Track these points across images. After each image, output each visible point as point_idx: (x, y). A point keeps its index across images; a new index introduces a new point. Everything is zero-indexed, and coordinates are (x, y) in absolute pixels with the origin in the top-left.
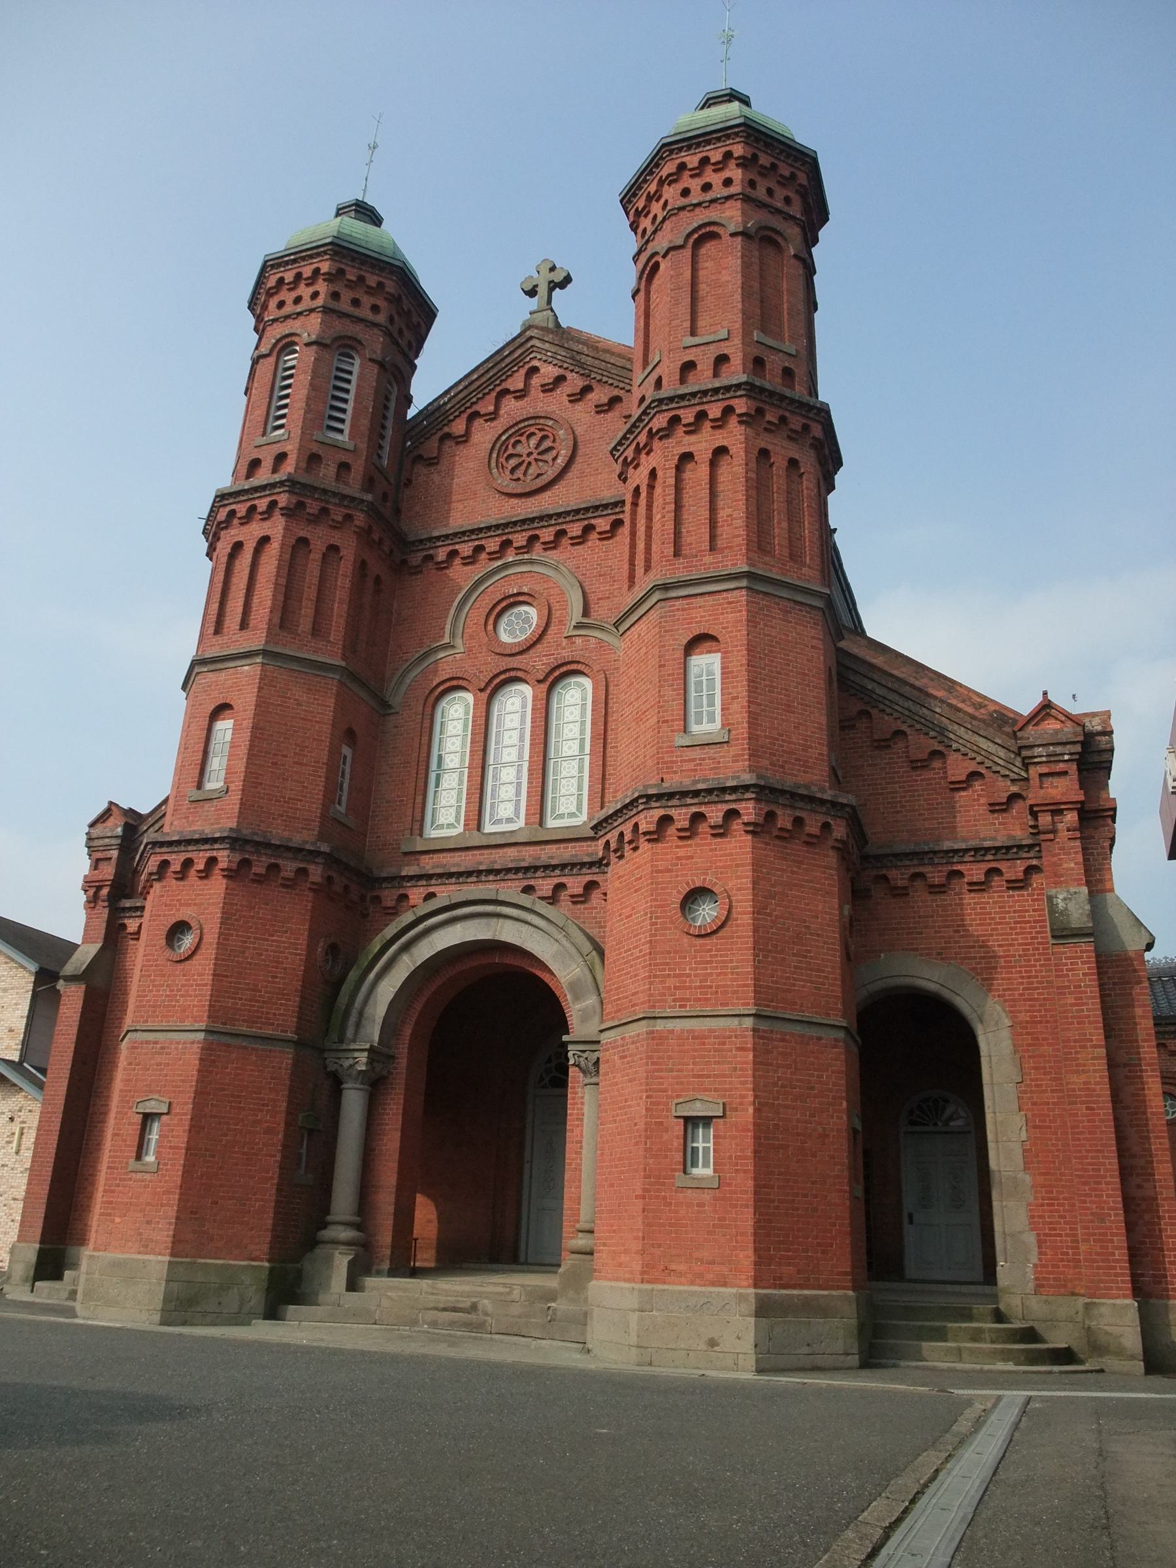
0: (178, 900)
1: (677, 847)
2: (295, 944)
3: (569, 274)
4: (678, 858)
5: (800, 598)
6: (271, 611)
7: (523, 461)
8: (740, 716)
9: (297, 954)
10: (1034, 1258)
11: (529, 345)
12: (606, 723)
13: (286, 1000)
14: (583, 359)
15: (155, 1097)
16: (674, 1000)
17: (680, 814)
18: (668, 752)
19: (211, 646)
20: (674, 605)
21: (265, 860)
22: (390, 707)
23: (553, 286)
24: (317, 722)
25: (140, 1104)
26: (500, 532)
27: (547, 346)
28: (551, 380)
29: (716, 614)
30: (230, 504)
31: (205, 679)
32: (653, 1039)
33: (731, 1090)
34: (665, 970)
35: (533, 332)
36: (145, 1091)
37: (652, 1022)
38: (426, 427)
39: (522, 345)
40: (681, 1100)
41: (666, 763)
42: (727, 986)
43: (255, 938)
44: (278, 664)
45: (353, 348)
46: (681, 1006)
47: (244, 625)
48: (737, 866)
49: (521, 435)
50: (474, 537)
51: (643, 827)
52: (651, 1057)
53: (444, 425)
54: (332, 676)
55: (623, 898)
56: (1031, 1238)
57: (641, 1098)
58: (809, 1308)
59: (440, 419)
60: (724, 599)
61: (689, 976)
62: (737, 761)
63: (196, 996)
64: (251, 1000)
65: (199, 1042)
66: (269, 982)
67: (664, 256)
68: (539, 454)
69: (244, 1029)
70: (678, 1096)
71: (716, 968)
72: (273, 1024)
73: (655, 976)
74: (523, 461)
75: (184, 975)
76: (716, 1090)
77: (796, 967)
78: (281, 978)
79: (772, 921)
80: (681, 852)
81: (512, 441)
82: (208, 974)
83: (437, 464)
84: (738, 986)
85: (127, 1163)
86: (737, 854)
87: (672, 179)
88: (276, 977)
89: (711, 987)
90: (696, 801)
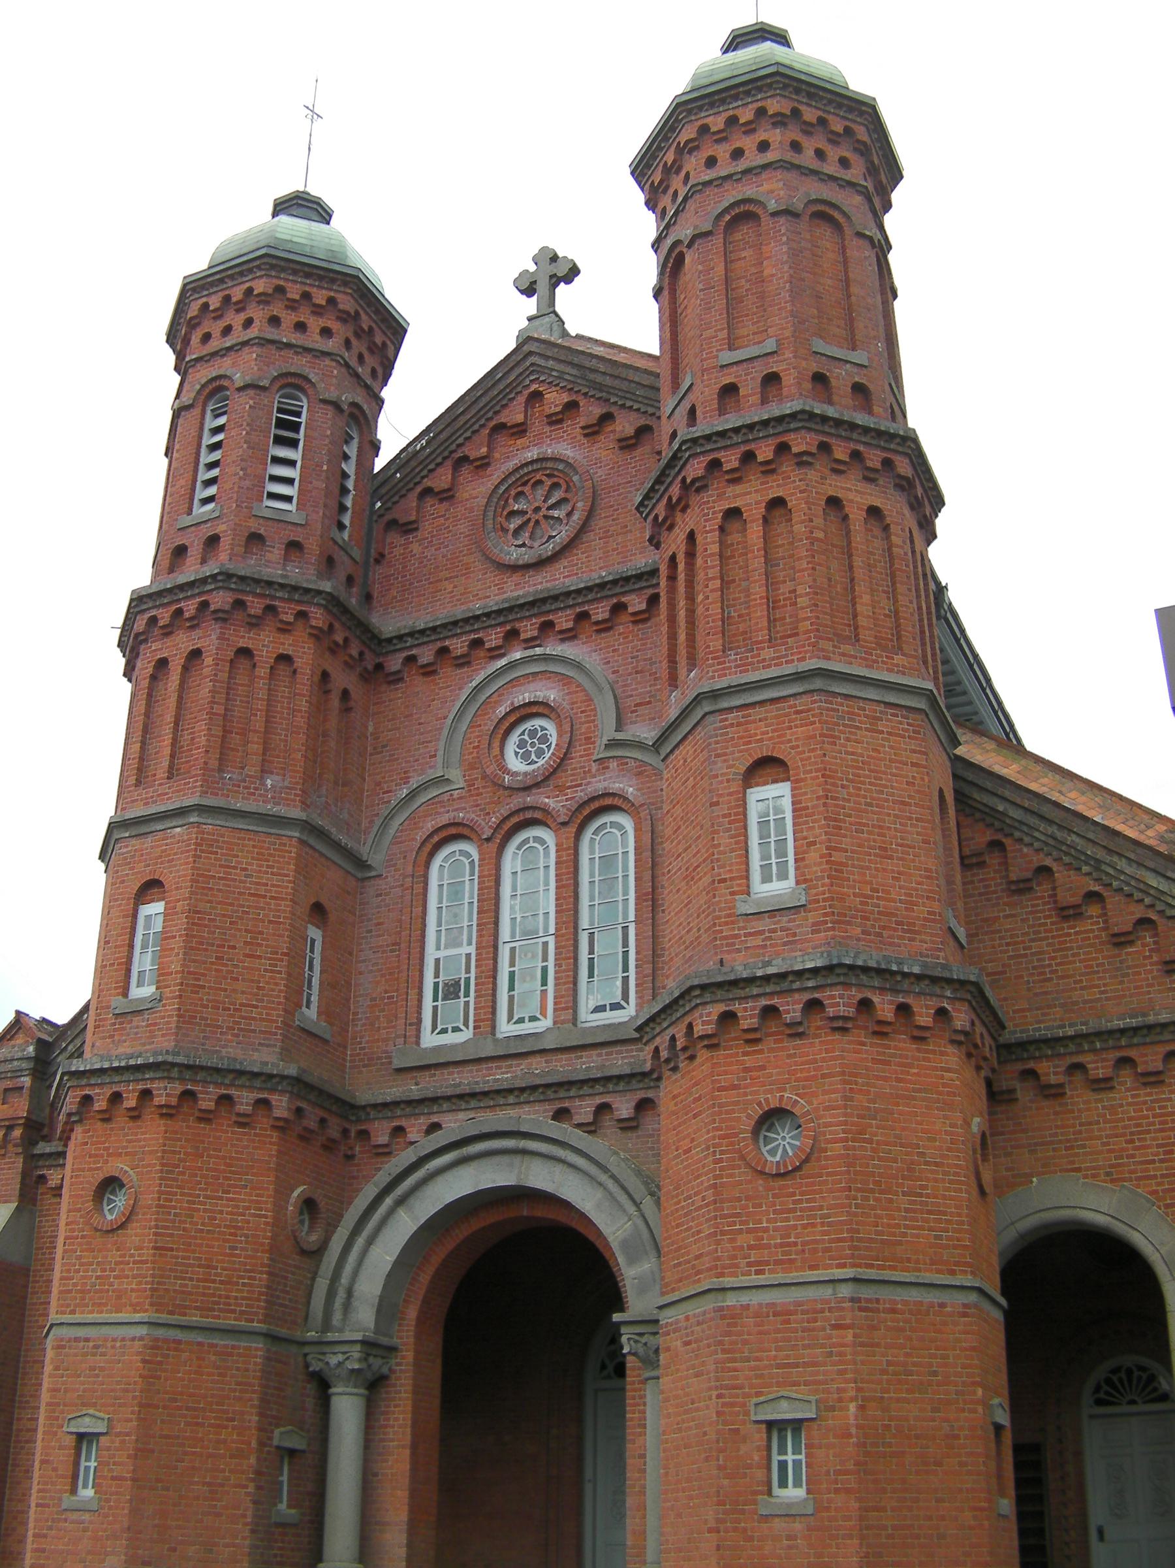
1: (745, 1054)
2: (258, 1202)
3: (575, 264)
4: (746, 1070)
5: (891, 698)
7: (529, 520)
13: (250, 1278)
14: (599, 378)
15: (91, 1411)
16: (749, 1264)
17: (745, 1010)
18: (726, 923)
19: (133, 801)
20: (726, 719)
21: (214, 1091)
22: (369, 868)
23: (555, 281)
24: (272, 898)
25: (73, 1422)
26: (502, 619)
27: (551, 363)
28: (559, 409)
29: (783, 729)
30: (148, 609)
31: (127, 846)
32: (723, 1317)
33: (825, 1382)
34: (734, 1223)
35: (533, 347)
36: (76, 1405)
37: (720, 1296)
38: (401, 480)
39: (518, 364)
40: (762, 1399)
41: (726, 938)
42: (816, 1242)
43: (206, 1197)
44: (218, 822)
46: (758, 1272)
48: (824, 1076)
49: (525, 484)
50: (468, 628)
51: (699, 1029)
52: (721, 1343)
53: (423, 478)
54: (289, 833)
55: (680, 1125)
57: (710, 1399)
59: (417, 470)
60: (790, 707)
61: (766, 1230)
62: (818, 931)
63: (134, 1277)
64: (205, 1280)
65: (141, 1339)
66: (225, 1255)
67: (689, 246)
68: (549, 508)
69: (195, 1319)
70: (758, 1394)
71: (801, 1218)
72: (234, 1311)
73: (723, 1233)
74: (529, 520)
75: (118, 1250)
77: (907, 1210)
78: (242, 1249)
79: (874, 1150)
80: (749, 1061)
81: (513, 493)
83: (416, 529)
84: (831, 1241)
85: (60, 1499)
86: (823, 1060)
87: (691, 147)
89: (795, 1244)
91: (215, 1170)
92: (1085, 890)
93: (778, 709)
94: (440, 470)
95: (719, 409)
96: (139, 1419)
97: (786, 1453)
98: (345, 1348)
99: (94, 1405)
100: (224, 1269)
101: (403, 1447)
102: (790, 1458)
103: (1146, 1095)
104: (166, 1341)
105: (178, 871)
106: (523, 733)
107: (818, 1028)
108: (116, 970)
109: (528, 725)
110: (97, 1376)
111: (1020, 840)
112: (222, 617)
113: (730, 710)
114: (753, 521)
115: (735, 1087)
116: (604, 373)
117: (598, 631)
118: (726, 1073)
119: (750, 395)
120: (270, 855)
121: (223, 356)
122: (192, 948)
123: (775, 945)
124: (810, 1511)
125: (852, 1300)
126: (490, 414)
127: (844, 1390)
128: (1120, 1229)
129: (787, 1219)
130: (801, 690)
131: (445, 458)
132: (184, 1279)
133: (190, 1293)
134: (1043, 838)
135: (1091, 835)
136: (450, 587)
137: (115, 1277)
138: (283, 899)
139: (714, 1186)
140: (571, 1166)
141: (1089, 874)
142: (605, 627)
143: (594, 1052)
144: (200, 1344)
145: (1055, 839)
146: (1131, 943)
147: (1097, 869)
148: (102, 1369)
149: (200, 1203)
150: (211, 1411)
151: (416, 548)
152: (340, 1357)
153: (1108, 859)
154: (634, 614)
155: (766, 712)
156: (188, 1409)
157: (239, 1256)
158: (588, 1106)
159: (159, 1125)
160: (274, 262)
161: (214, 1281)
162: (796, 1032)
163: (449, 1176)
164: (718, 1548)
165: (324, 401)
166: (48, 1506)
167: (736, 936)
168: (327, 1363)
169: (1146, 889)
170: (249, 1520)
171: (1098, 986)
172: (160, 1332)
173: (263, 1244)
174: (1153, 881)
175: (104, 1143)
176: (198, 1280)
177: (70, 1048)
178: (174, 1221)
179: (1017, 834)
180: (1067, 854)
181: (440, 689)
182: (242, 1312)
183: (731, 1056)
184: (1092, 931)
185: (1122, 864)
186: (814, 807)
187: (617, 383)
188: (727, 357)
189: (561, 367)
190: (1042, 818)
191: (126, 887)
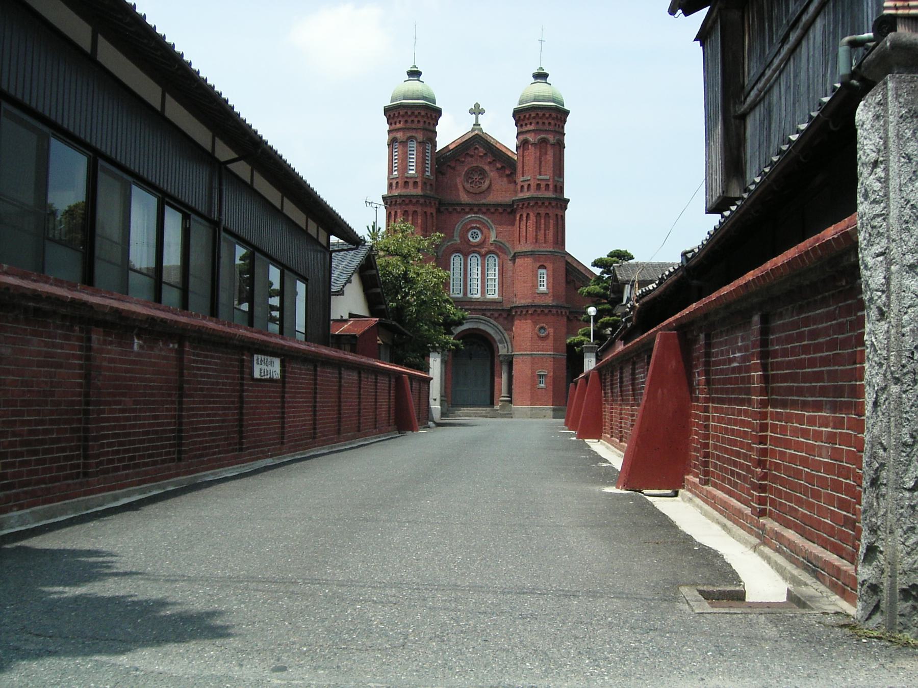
35: (478, 136)
51: (530, 312)
109: (475, 230)
142: (493, 213)
162: (546, 315)
188: (539, 177)
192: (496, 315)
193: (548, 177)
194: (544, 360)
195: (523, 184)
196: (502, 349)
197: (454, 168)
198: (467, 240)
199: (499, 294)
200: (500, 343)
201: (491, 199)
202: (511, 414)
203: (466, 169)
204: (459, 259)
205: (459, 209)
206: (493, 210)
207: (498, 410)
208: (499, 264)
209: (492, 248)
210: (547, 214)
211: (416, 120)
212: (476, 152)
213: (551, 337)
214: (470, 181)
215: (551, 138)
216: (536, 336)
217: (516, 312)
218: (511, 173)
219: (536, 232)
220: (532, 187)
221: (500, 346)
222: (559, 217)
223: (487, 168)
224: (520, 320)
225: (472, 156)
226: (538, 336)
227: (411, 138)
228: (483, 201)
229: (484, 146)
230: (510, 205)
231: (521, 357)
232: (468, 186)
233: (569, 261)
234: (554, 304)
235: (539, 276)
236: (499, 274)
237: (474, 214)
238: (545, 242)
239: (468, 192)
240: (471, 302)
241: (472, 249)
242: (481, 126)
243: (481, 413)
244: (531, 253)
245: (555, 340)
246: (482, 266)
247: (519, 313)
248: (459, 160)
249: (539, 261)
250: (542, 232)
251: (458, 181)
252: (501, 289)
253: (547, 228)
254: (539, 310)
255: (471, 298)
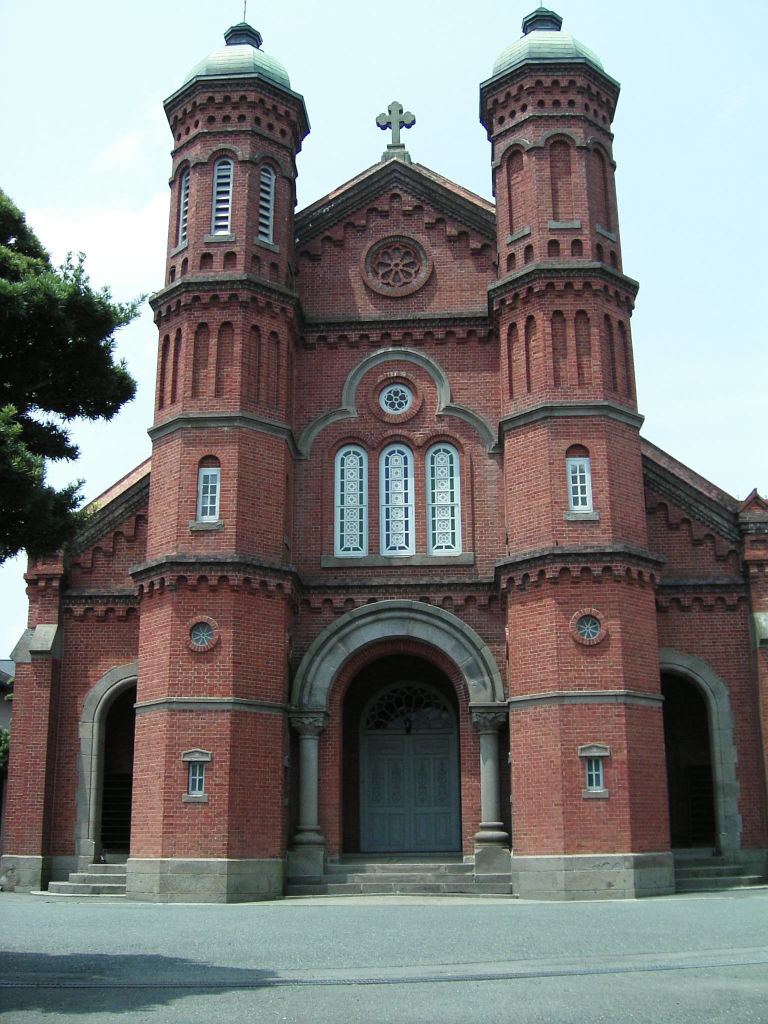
0: (196, 606)
1: (571, 588)
2: (277, 638)
5: (630, 422)
6: (241, 385)
7: (392, 270)
8: (605, 504)
9: (279, 646)
10: (740, 829)
11: (392, 176)
12: (472, 482)
15: (199, 750)
16: (575, 686)
17: (574, 568)
18: (559, 523)
19: (191, 407)
20: (557, 422)
23: (402, 124)
24: (275, 472)
27: (407, 180)
31: (189, 433)
33: (613, 740)
34: (568, 666)
39: (387, 175)
40: (584, 746)
41: (558, 531)
43: (255, 635)
45: (270, 165)
46: (579, 690)
47: (218, 393)
49: (388, 248)
51: (549, 575)
52: (563, 721)
54: (280, 436)
55: (527, 616)
56: (739, 818)
58: (656, 862)
61: (583, 670)
62: (605, 533)
63: (220, 678)
64: (256, 680)
65: (228, 711)
66: (265, 666)
68: (403, 266)
69: (253, 700)
70: (581, 744)
71: (600, 666)
72: (269, 696)
74: (392, 270)
76: (604, 740)
77: (641, 665)
78: (271, 663)
79: (630, 637)
80: (573, 592)
81: (381, 251)
82: (229, 663)
83: (320, 260)
84: (614, 677)
86: (609, 594)
88: (269, 663)
89: (597, 678)
90: (584, 559)
91: (258, 621)
92: (682, 517)
93: (584, 421)
94: (336, 228)
95: (549, 252)
96: (230, 754)
97: (592, 771)
98: (315, 715)
99: (200, 747)
100: (264, 674)
101: (335, 766)
102: (594, 773)
103: (705, 615)
104: (240, 712)
105: (229, 453)
106: (390, 392)
107: (607, 579)
108: (189, 505)
109: (399, 388)
110: (200, 731)
111: (653, 489)
112: (244, 305)
113: (559, 417)
114: (570, 320)
115: (568, 603)
116: (441, 195)
117: (437, 344)
118: (562, 596)
119: (567, 249)
120: (273, 447)
121: (226, 136)
122: (240, 498)
123: (583, 537)
124: (607, 796)
125: (625, 704)
126: (368, 201)
127: (622, 744)
128: (691, 674)
129: (594, 666)
130: (596, 414)
131: (339, 221)
132: (247, 679)
133: (250, 687)
134: (663, 489)
135: (688, 492)
136: (343, 300)
137: (207, 677)
138: (279, 473)
139: (557, 648)
140: (437, 627)
141: (685, 510)
142: (441, 342)
143: (439, 570)
144: (255, 713)
145: (670, 491)
146: (701, 545)
147: (690, 508)
148: (204, 727)
149: (252, 638)
150: (262, 749)
151: (319, 270)
152: (311, 720)
153: (695, 504)
154: (458, 339)
155: (578, 421)
156: (252, 748)
157: (270, 667)
158: (440, 597)
159: (231, 596)
160: (261, 83)
161: (260, 681)
162: (597, 580)
163: (367, 628)
164: (563, 813)
165: (284, 177)
166: (173, 801)
167: (564, 531)
168: (303, 723)
169: (712, 521)
170: (280, 804)
171: (685, 563)
172: (237, 708)
173: (280, 661)
174: (716, 518)
175: (193, 603)
176: (253, 680)
177: (86, 534)
178: (241, 648)
179: (651, 486)
180: (674, 499)
181: (340, 358)
182: (273, 697)
183: (564, 588)
184: (683, 536)
185: (702, 508)
186: (603, 473)
187: (449, 203)
188: (553, 225)
189: (414, 184)
190: (665, 480)
191: (191, 457)
192: (458, 598)
193: (577, 224)
194: (599, 712)
195: (512, 250)
196: (478, 691)
197: (340, 244)
198: (375, 410)
199: (464, 544)
200: (472, 676)
201: (436, 308)
202: (509, 878)
203: (370, 244)
204: (356, 460)
205: (353, 336)
206: (440, 334)
207: (470, 868)
208: (461, 467)
209: (442, 427)
210: (581, 313)
211: (234, 115)
212: (395, 205)
213: (616, 647)
214: (381, 273)
215: (578, 135)
216: (571, 643)
217: (511, 580)
218: (485, 247)
219: (556, 361)
220: (536, 251)
221: (472, 683)
222: (615, 325)
223: (422, 238)
224: (523, 603)
225: (385, 215)
226: (579, 644)
227: (221, 156)
228: (420, 315)
229: (413, 189)
230: (484, 319)
231: (531, 710)
232: (377, 284)
233: (649, 453)
234: (619, 548)
235: (570, 475)
236: (462, 494)
237: (394, 346)
238: (581, 384)
239: (376, 296)
240: (390, 567)
241: (390, 432)
242: (407, 149)
243: (422, 879)
244: (541, 415)
245: (628, 652)
246: (416, 476)
247: (518, 582)
248: (352, 225)
249: (568, 435)
250: (572, 358)
251: (354, 274)
252: (469, 530)
253: (583, 349)
254: (575, 569)
255: (390, 558)
